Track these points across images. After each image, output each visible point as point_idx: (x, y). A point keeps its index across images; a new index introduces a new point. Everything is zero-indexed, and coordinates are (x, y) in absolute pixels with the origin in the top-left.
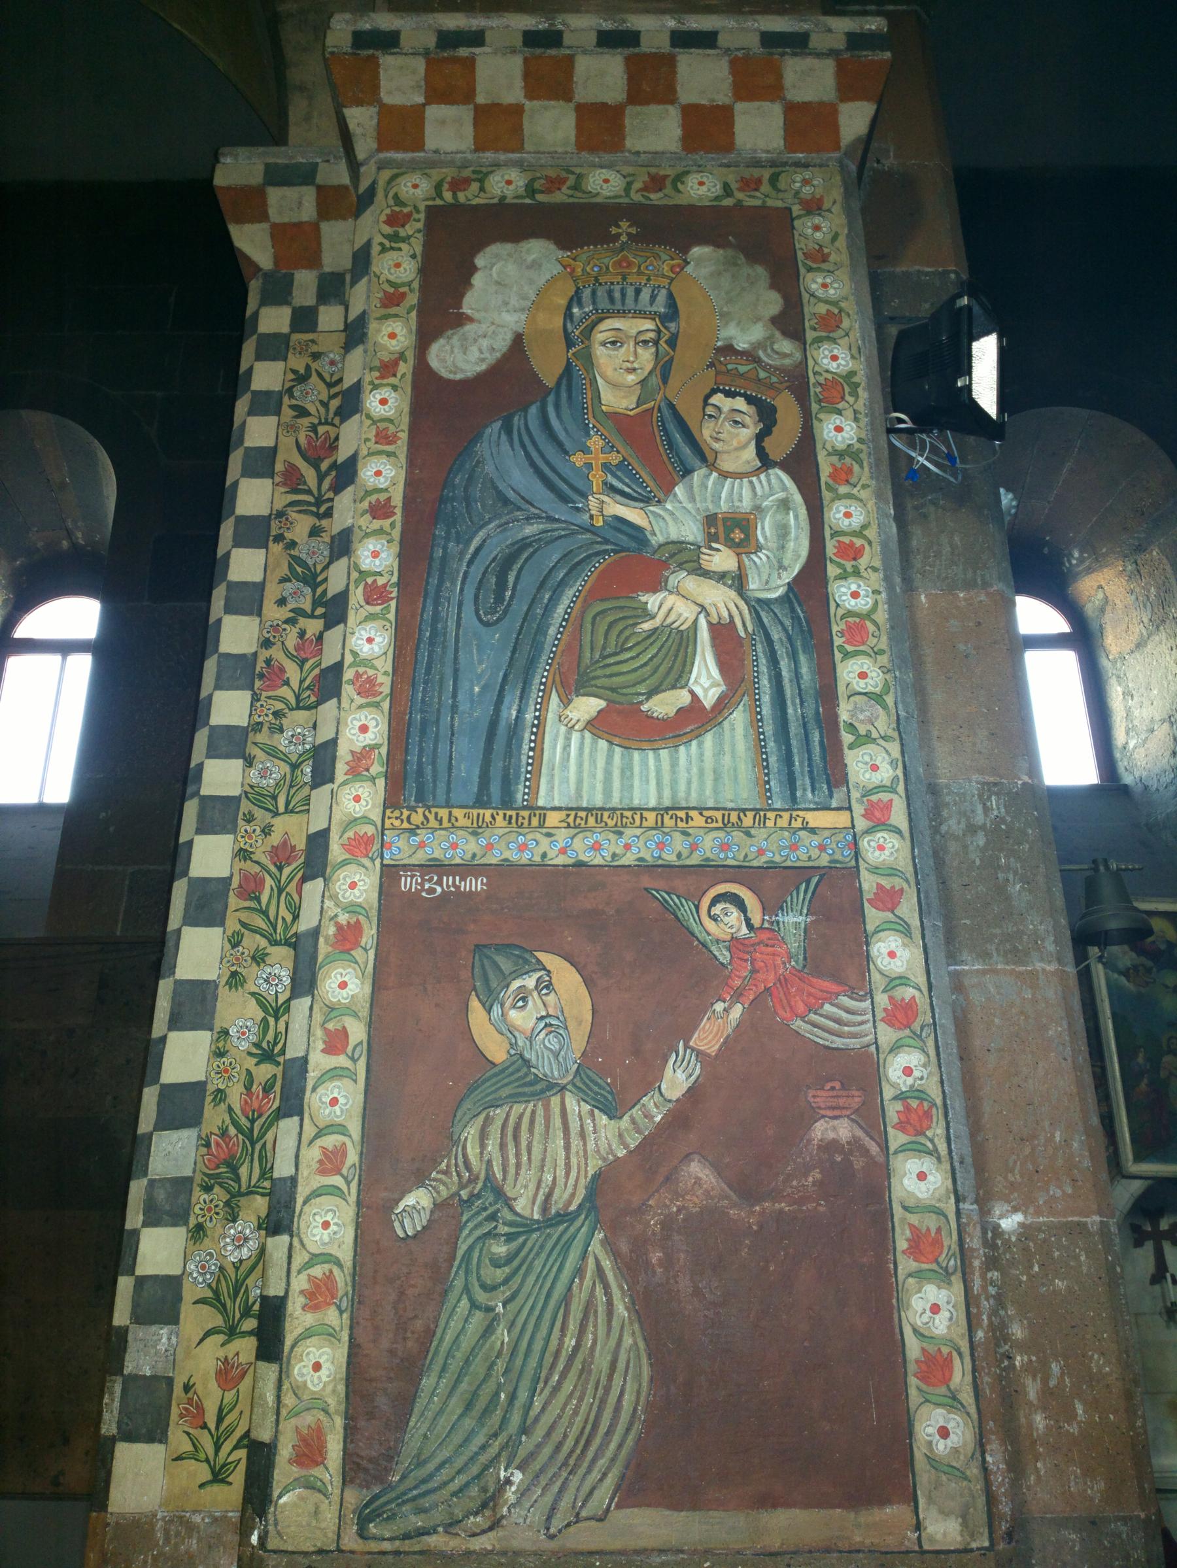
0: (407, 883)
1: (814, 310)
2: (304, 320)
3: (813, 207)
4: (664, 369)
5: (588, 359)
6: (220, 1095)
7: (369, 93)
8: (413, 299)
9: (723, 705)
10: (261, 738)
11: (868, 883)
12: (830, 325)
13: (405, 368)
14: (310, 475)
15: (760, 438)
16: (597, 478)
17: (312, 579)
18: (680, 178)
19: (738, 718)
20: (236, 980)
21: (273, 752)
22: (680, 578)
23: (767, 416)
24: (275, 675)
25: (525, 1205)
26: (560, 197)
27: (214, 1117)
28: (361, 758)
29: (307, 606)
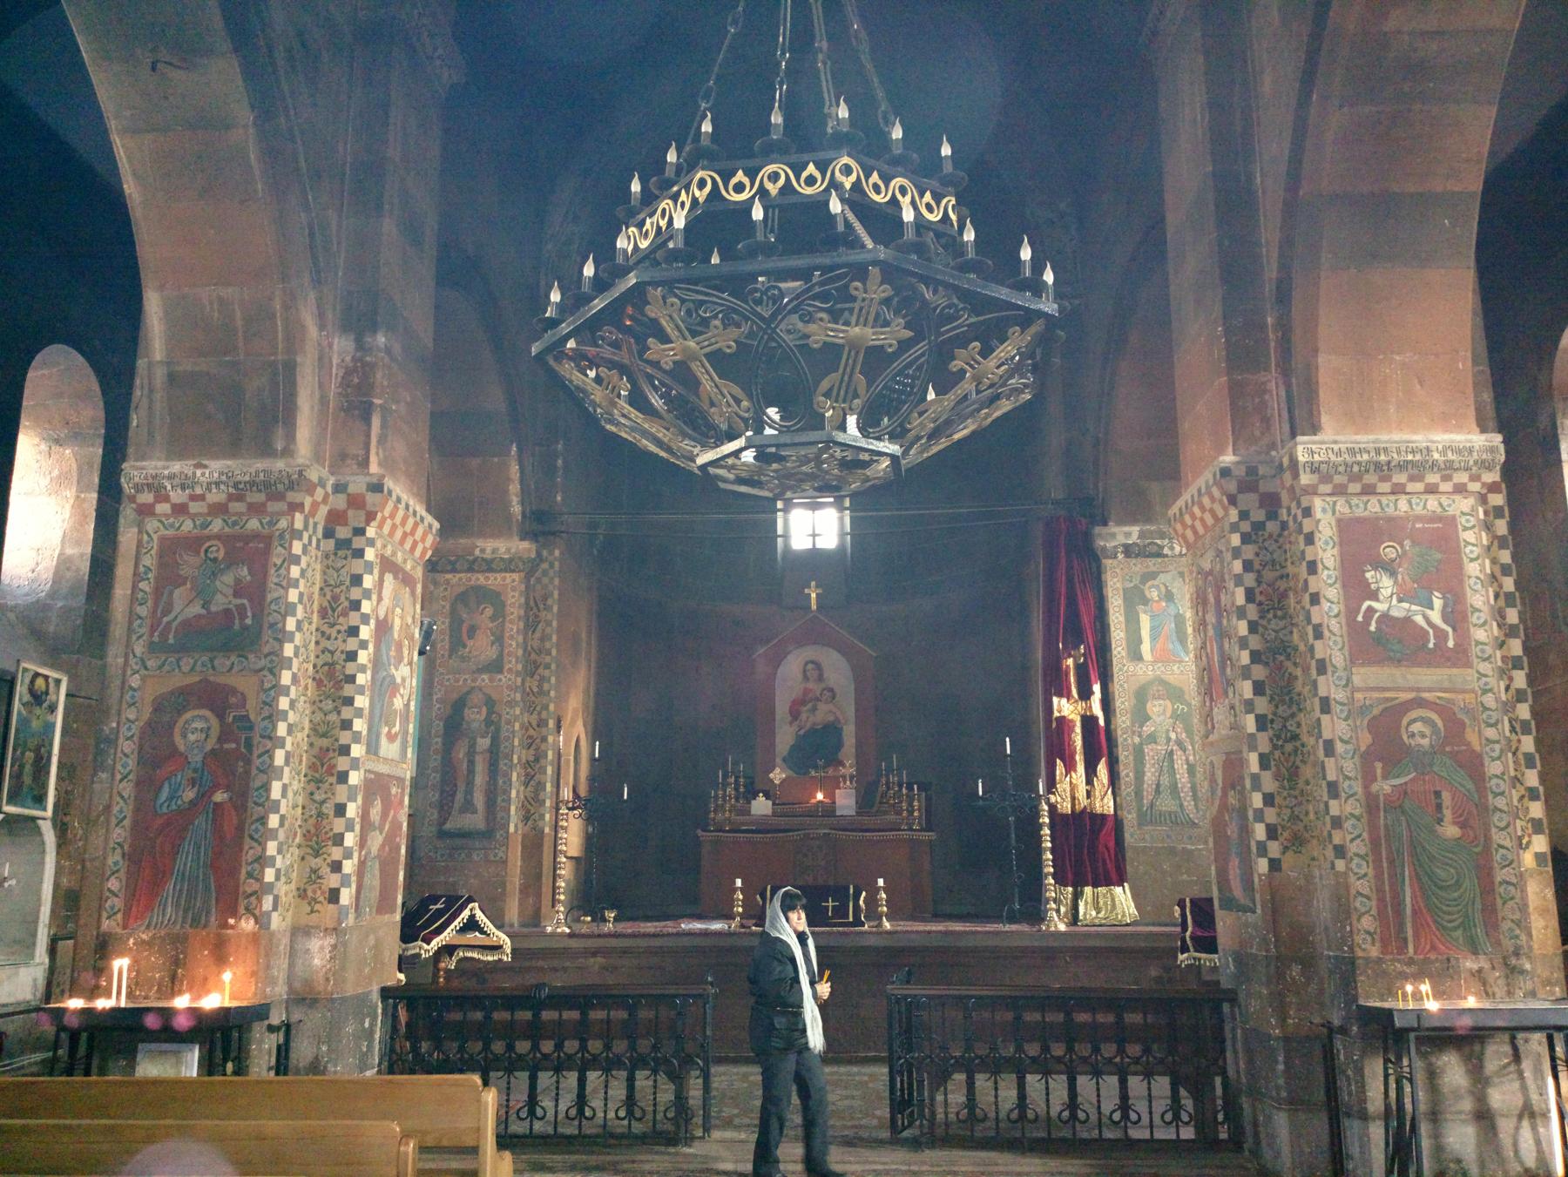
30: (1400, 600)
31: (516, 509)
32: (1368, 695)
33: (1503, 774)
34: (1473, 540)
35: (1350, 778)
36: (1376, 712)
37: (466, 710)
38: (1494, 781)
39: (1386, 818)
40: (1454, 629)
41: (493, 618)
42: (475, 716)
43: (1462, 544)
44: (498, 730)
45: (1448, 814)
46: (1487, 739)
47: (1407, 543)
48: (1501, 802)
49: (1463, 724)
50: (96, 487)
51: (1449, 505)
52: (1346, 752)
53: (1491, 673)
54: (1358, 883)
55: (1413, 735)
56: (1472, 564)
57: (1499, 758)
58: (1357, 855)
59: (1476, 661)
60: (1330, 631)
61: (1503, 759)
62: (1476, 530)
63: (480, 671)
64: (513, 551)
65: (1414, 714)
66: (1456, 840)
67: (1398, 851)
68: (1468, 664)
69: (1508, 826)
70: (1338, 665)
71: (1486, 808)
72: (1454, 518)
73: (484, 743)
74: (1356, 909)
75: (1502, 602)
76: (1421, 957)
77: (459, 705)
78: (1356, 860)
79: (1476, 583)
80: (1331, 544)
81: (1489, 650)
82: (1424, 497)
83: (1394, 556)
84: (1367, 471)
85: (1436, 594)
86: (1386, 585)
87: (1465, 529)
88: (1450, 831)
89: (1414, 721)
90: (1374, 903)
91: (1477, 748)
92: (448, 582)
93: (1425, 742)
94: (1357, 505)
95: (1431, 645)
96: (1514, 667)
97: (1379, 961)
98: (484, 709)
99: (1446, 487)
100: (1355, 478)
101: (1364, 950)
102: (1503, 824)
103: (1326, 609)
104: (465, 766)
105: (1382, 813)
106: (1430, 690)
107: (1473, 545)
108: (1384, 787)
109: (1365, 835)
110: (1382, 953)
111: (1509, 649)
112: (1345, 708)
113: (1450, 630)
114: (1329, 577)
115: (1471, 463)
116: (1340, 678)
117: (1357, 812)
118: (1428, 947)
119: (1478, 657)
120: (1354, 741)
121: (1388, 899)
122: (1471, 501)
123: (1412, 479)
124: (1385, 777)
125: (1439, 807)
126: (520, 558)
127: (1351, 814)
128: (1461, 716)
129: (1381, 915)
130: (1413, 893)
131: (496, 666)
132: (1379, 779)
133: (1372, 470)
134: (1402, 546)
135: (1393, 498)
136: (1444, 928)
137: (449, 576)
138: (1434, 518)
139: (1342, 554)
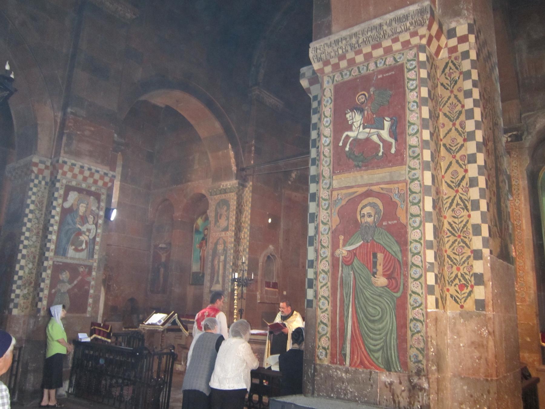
0: (55, 263)
1: (101, 207)
2: (40, 182)
3: (103, 194)
4: (86, 211)
5: (79, 208)
6: (24, 277)
7: (62, 168)
8: (62, 197)
9: (85, 249)
10: (31, 238)
11: (93, 267)
12: (102, 209)
13: (61, 205)
14: (39, 205)
15: (94, 220)
16: (78, 222)
17: (37, 219)
18: (91, 187)
19: (86, 250)
20: (26, 266)
21: (32, 240)
22: (84, 235)
23: (94, 218)
24: (32, 231)
25: (62, 291)
26: (79, 186)
27: (23, 279)
28: (52, 250)
29: (37, 222)
30: (364, 128)
31: (234, 168)
32: (339, 192)
33: (420, 239)
34: (414, 77)
35: (324, 247)
36: (344, 203)
37: (218, 246)
38: (414, 245)
39: (342, 271)
40: (396, 140)
41: (226, 211)
42: (220, 248)
43: (406, 81)
44: (226, 253)
45: (380, 268)
46: (411, 215)
47: (372, 89)
48: (417, 260)
49: (395, 205)
50: (119, 180)
51: (400, 58)
52: (325, 230)
53: (417, 166)
54: (322, 315)
55: (363, 216)
56: (412, 93)
57: (418, 228)
58: (323, 297)
59: (408, 159)
60: (324, 155)
61: (421, 228)
62: (416, 69)
63: (223, 231)
64: (231, 184)
65: (365, 202)
66: (383, 287)
67: (347, 294)
68: (402, 162)
69: (421, 276)
70: (326, 176)
71: (406, 264)
72: (402, 65)
73: (222, 258)
74: (319, 332)
75: (463, 117)
76: (354, 369)
77: (216, 244)
78: (323, 300)
79: (413, 106)
80: (330, 101)
81: (418, 150)
82: (384, 58)
83: (363, 100)
84: (347, 51)
85: (387, 119)
86: (356, 119)
87: (409, 70)
88: (381, 281)
89: (365, 206)
90: (329, 329)
91: (403, 220)
92: (215, 199)
93: (370, 220)
94: (346, 74)
95: (380, 154)
96: (469, 162)
97: (328, 368)
98: (223, 246)
99: (397, 46)
100: (342, 57)
101: (320, 359)
102: (416, 276)
103: (323, 142)
104: (217, 266)
105: (340, 269)
106: (378, 184)
107: (413, 80)
108: (343, 251)
109: (329, 284)
110: (331, 363)
111: (466, 150)
112: (327, 202)
113: (393, 141)
114: (327, 122)
115: (408, 24)
116: (326, 184)
117: (326, 269)
118: (358, 362)
119: (410, 157)
120: (330, 223)
121: (338, 327)
122: (414, 51)
123: (375, 47)
124: (344, 245)
125: (375, 264)
126: (234, 187)
127: (323, 270)
128: (396, 199)
129: (333, 338)
130: (353, 323)
131: (226, 229)
132: (341, 245)
133: (349, 50)
134: (368, 92)
135: (366, 64)
136: (371, 350)
137: (215, 197)
138: (391, 69)
139: (335, 105)
